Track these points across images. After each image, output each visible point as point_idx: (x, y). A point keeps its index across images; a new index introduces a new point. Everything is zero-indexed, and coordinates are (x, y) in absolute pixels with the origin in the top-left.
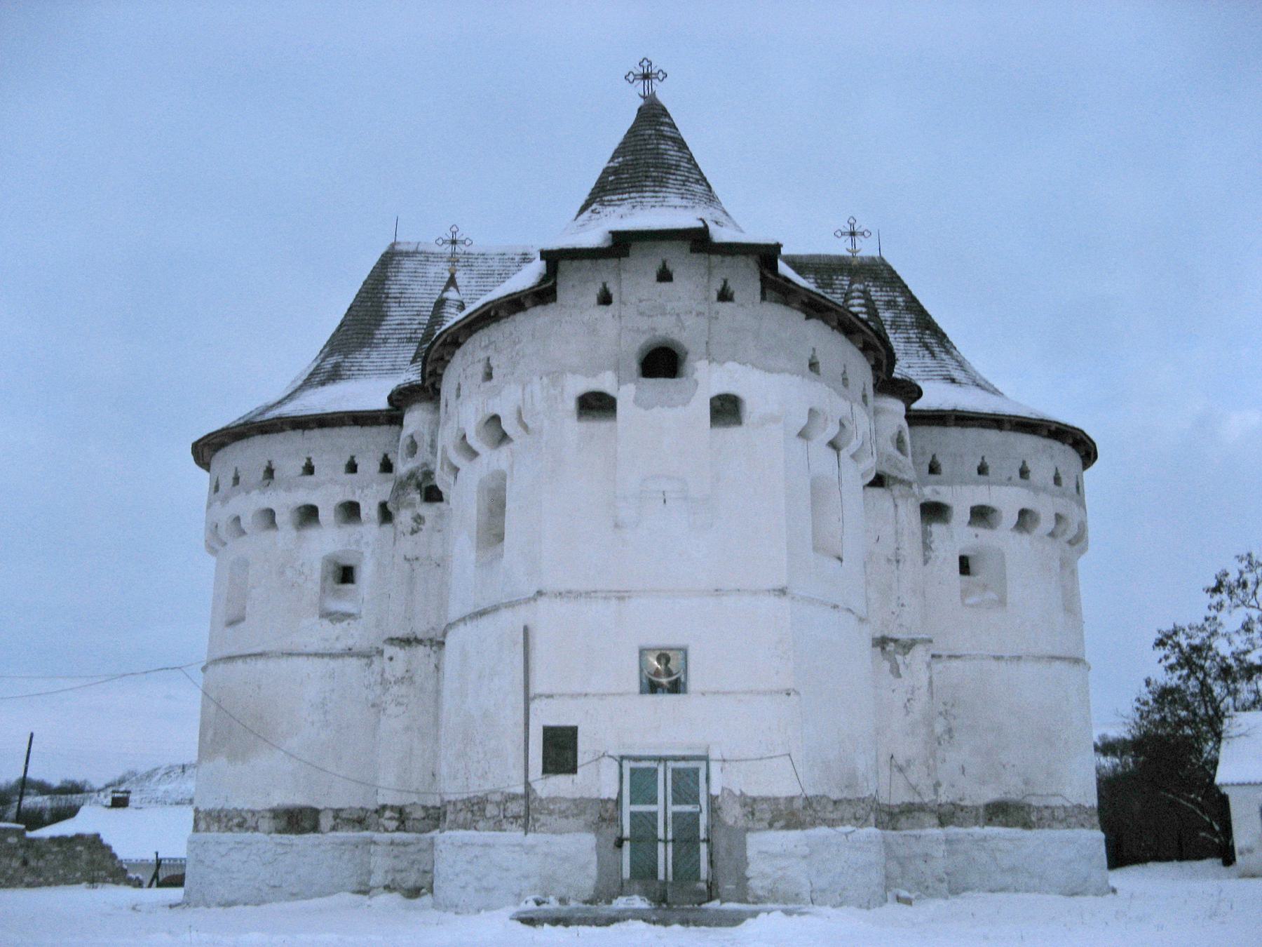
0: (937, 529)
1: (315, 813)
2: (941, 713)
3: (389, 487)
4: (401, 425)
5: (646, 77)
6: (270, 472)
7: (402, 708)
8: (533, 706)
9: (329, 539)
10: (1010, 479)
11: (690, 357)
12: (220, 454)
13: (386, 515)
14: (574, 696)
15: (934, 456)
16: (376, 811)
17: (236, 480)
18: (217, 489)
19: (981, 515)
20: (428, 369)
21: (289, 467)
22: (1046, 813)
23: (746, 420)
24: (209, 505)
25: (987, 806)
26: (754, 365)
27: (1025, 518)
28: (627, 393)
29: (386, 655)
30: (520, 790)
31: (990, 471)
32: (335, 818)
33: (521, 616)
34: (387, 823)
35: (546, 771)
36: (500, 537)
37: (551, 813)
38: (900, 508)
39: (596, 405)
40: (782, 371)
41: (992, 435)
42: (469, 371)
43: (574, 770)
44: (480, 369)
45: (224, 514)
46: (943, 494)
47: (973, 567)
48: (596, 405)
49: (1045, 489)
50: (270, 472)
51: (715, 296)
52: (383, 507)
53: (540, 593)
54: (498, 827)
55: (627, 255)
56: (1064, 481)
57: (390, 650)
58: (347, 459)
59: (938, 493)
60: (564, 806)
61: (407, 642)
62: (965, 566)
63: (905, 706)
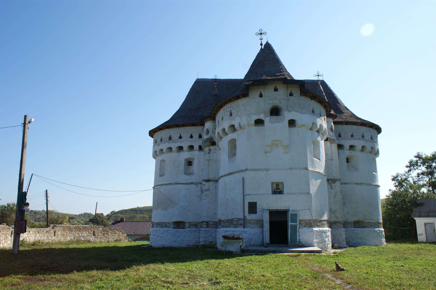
0: (341, 151)
1: (184, 223)
3: (202, 141)
4: (204, 126)
5: (261, 34)
6: (170, 138)
7: (207, 197)
8: (246, 197)
9: (186, 155)
11: (283, 110)
12: (156, 133)
13: (200, 148)
14: (256, 195)
16: (200, 223)
17: (161, 140)
18: (156, 142)
19: (352, 147)
20: (213, 113)
21: (175, 137)
22: (369, 224)
23: (297, 126)
24: (154, 146)
25: (354, 222)
26: (299, 112)
28: (267, 120)
29: (203, 184)
30: (242, 217)
31: (354, 136)
32: (190, 224)
33: (242, 175)
34: (204, 226)
35: (249, 213)
36: (235, 155)
37: (250, 223)
39: (259, 122)
40: (305, 114)
41: (355, 127)
42: (225, 114)
43: (256, 213)
44: (229, 113)
45: (158, 149)
46: (343, 142)
47: (349, 161)
48: (259, 122)
50: (170, 138)
51: (289, 94)
53: (247, 169)
54: (236, 226)
55: (267, 85)
57: (203, 183)
58: (190, 135)
60: (254, 221)
61: (208, 181)
62: (348, 160)
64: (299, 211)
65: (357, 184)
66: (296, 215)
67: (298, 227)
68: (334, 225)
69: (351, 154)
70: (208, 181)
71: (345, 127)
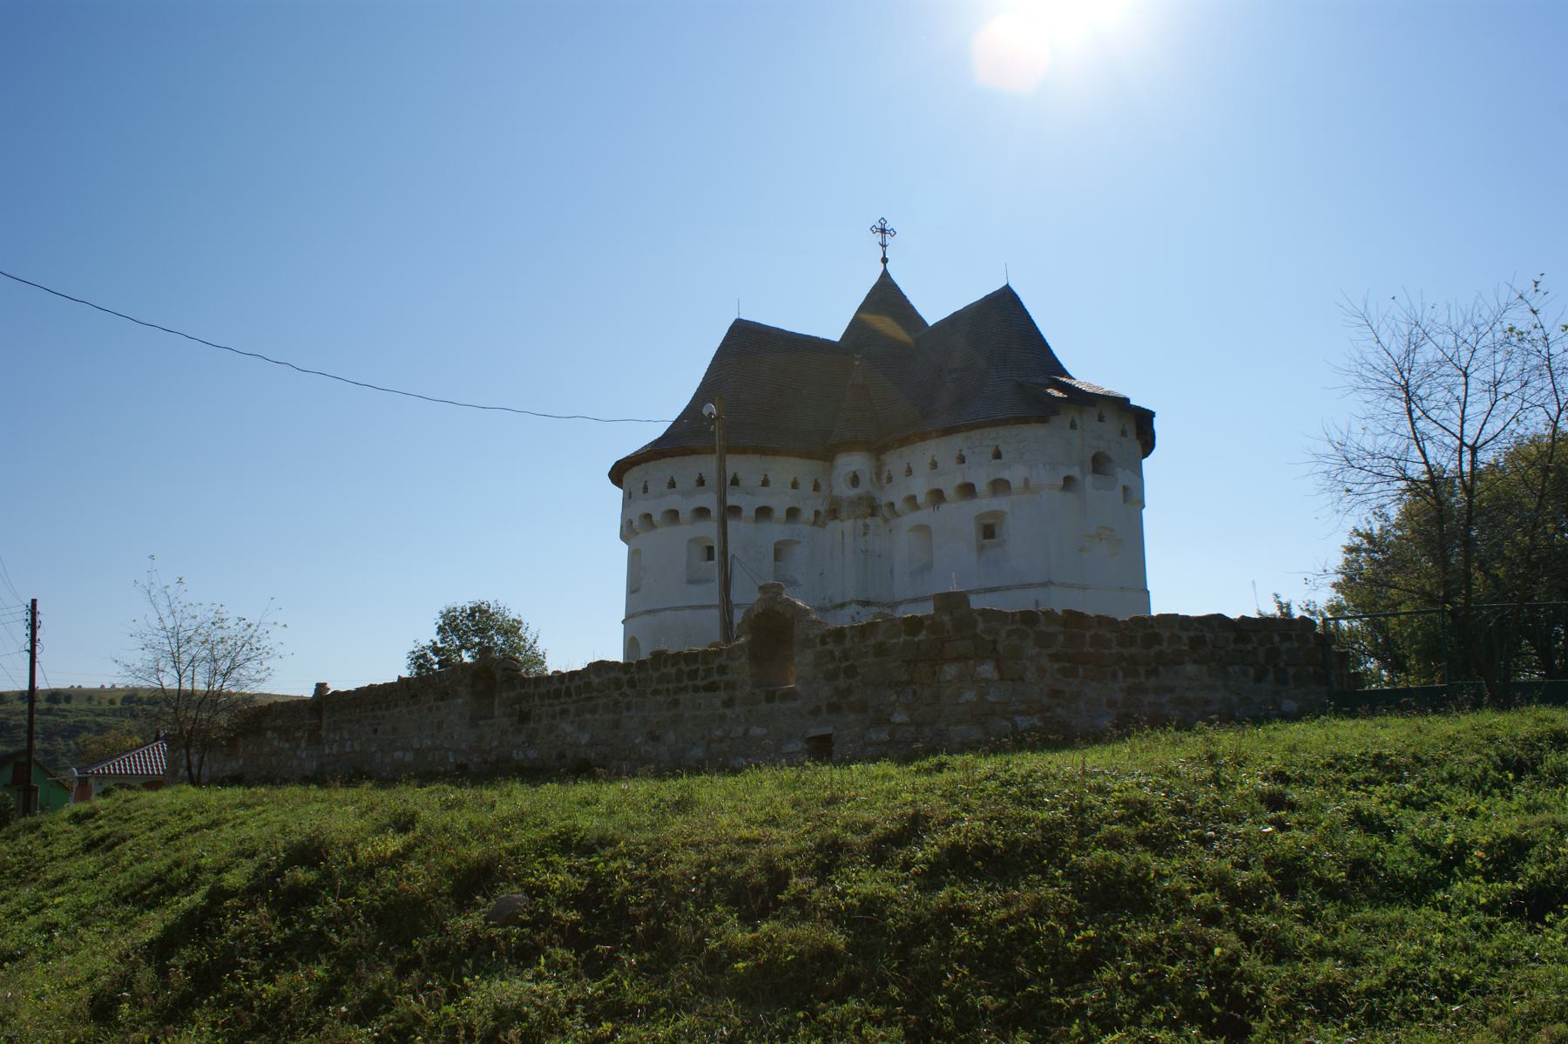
48: (1068, 482)
52: (817, 513)
58: (791, 479)
61: (866, 603)
70: (866, 603)
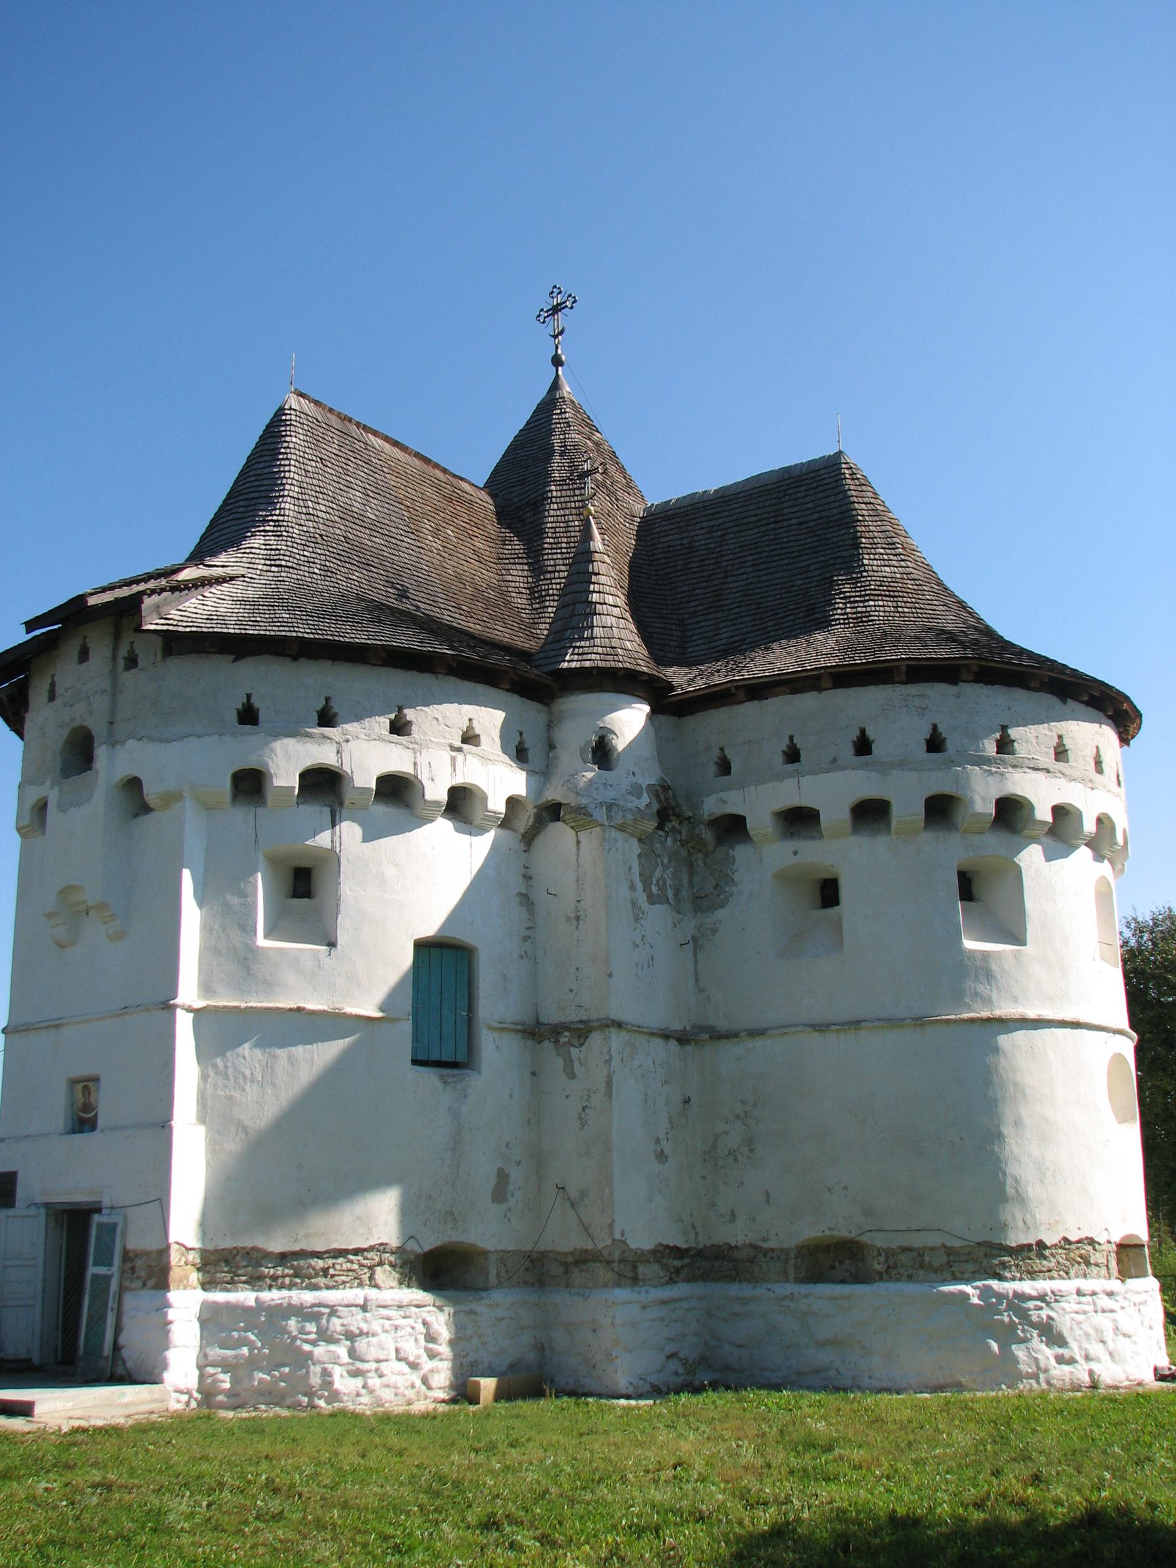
0: (741, 852)
2: (738, 1117)
10: (834, 760)
15: (722, 749)
19: (799, 820)
22: (904, 1258)
26: (150, 739)
27: (870, 814)
38: (583, 846)
40: (180, 739)
41: (808, 701)
46: (732, 802)
49: (902, 764)
51: (121, 663)
56: (952, 744)
59: (725, 802)
63: (580, 1118)
64: (130, 1211)
65: (821, 1027)
66: (114, 1226)
67: (114, 1285)
68: (576, 1272)
69: (794, 860)
71: (750, 709)
